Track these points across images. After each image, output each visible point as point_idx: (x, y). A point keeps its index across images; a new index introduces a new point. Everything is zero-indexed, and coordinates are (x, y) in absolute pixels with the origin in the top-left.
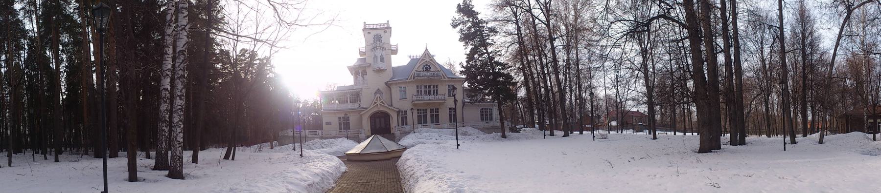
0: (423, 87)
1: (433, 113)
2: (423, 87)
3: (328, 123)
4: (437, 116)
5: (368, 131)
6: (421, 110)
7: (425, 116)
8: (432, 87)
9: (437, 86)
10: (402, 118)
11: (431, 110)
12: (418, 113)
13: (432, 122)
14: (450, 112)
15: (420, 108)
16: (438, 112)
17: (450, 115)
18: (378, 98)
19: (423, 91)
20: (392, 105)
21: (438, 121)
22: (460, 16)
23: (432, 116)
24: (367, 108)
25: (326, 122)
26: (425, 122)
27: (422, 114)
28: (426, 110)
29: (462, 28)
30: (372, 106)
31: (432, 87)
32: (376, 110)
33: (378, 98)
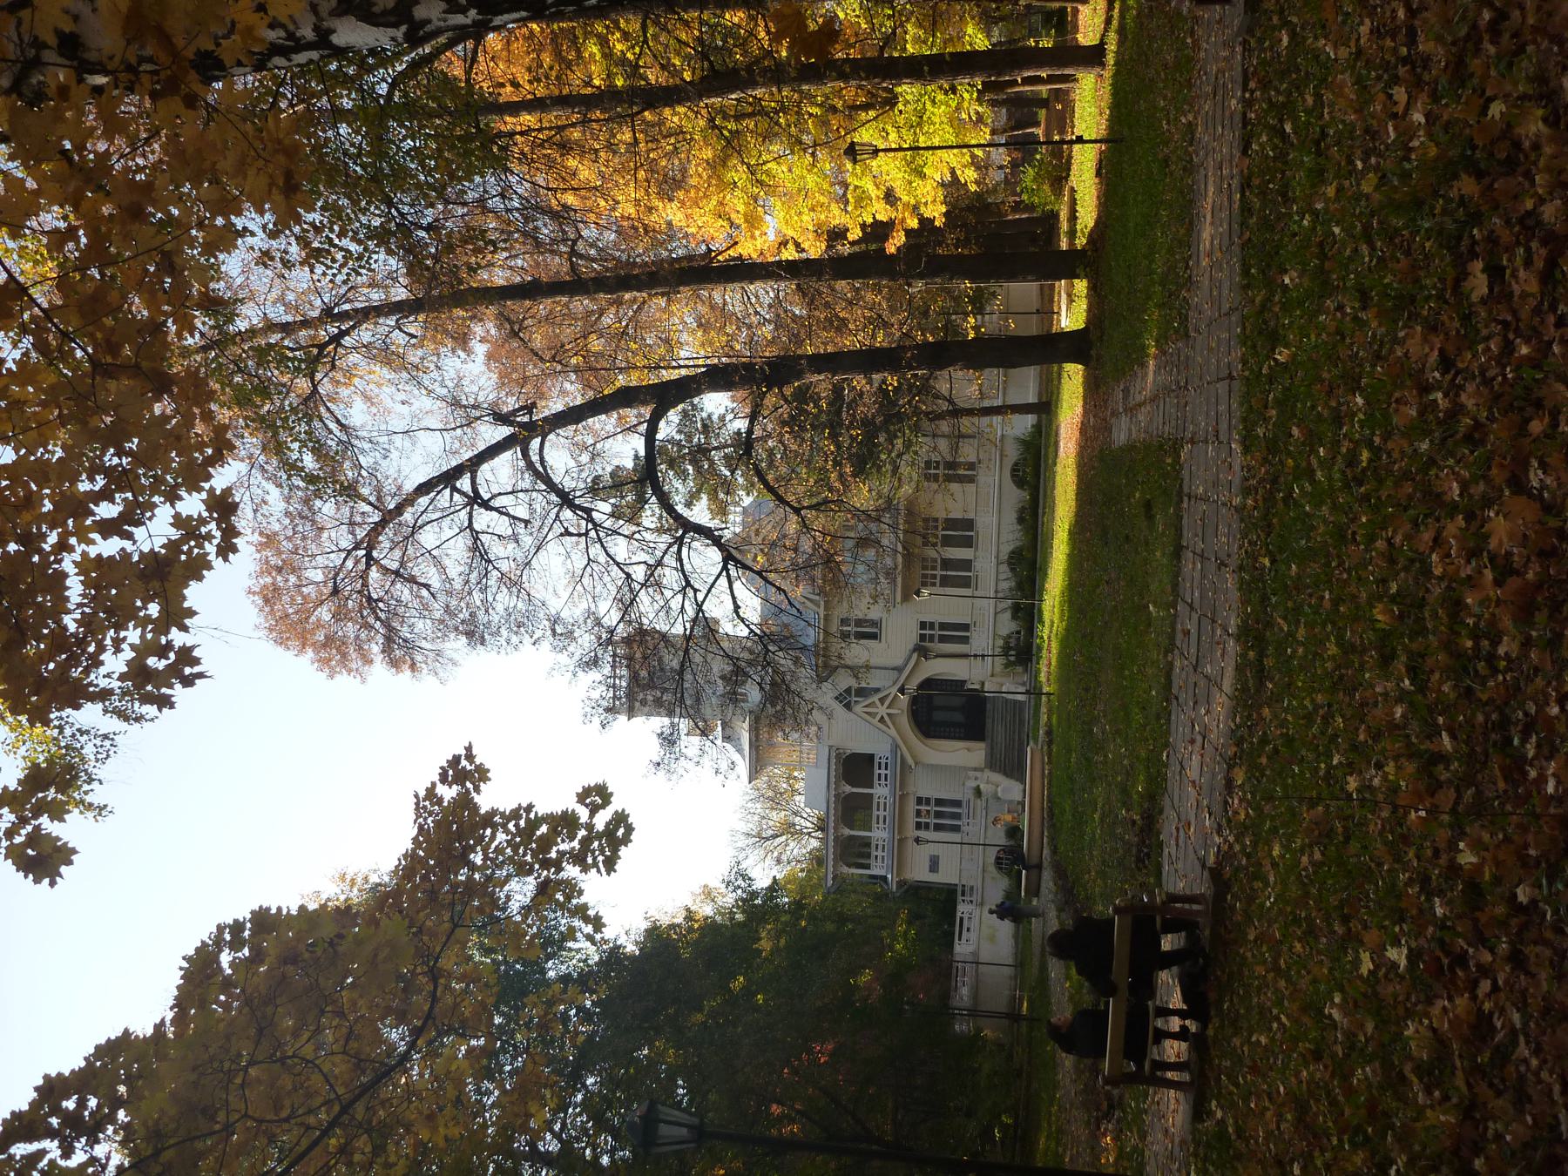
3: (934, 865)
4: (951, 523)
5: (968, 750)
10: (943, 639)
13: (968, 542)
16: (936, 520)
18: (866, 710)
20: (899, 670)
21: (969, 524)
23: (948, 542)
24: (897, 746)
26: (967, 565)
27: (939, 573)
30: (893, 732)
32: (904, 721)
33: (866, 710)
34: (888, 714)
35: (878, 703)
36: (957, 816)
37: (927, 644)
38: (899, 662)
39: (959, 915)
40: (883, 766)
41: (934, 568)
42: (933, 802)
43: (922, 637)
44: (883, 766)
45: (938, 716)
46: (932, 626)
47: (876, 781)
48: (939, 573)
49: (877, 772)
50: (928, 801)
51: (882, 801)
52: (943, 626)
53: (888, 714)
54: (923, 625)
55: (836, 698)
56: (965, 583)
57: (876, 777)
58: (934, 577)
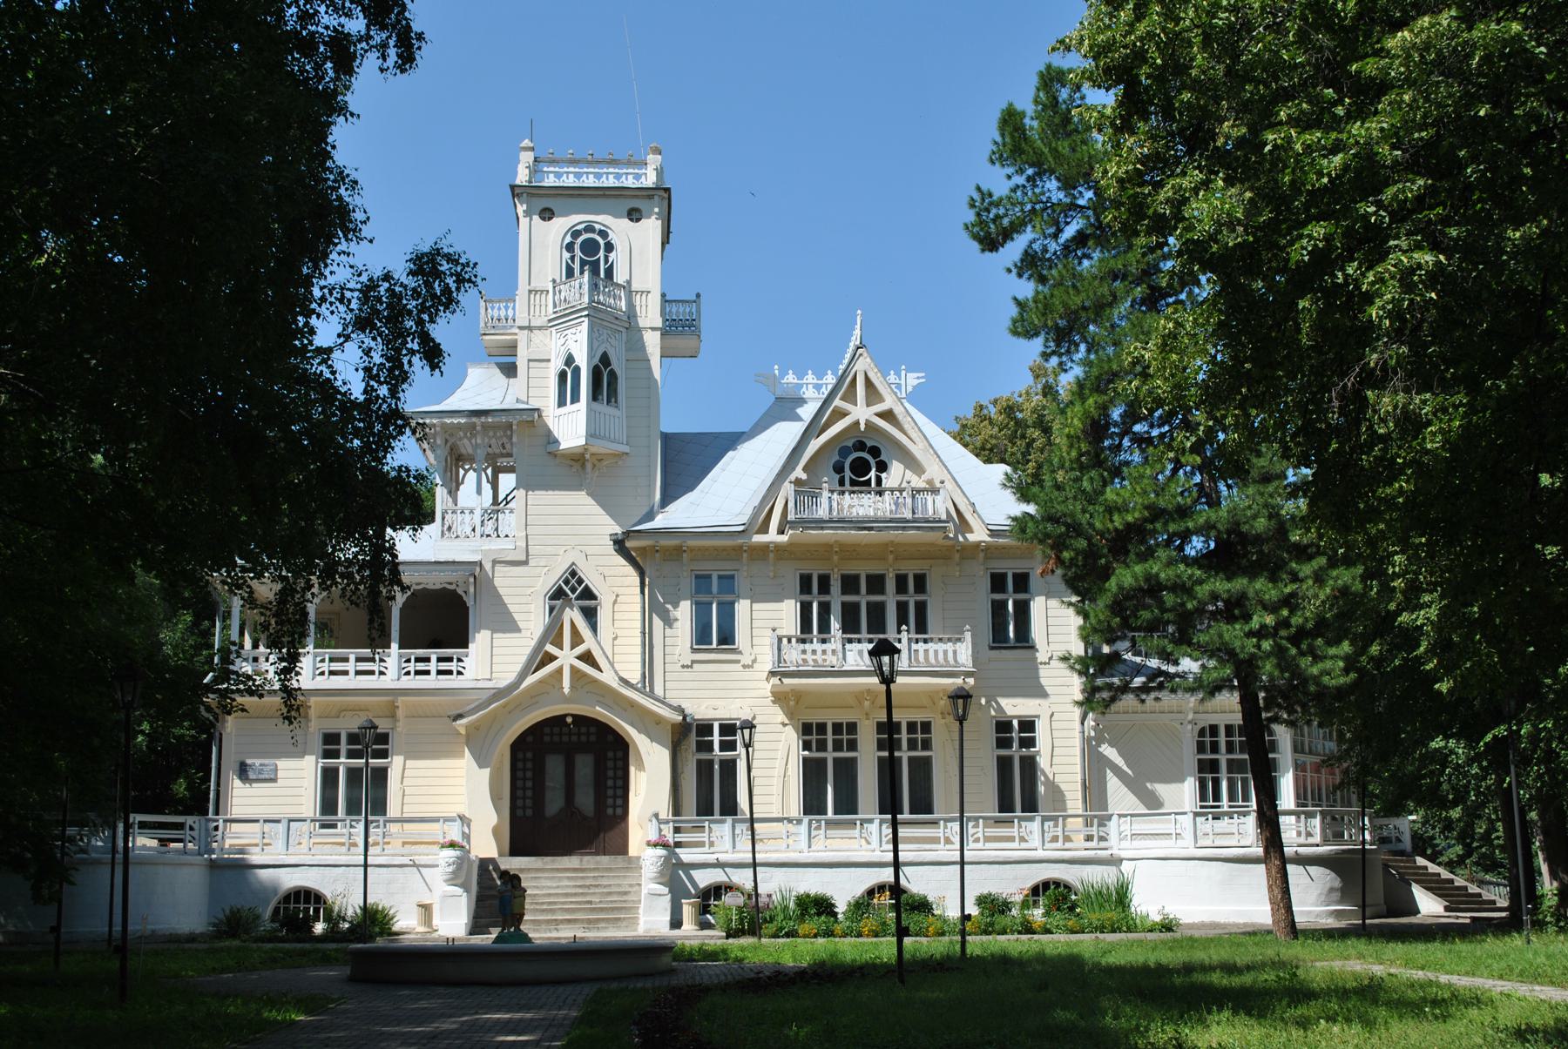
0: (836, 586)
2: (836, 586)
6: (822, 728)
7: (847, 772)
8: (890, 585)
9: (921, 585)
10: (704, 769)
12: (807, 746)
14: (1003, 743)
16: (927, 745)
17: (1004, 765)
19: (836, 609)
22: (1020, 180)
23: (889, 770)
26: (847, 804)
28: (852, 727)
29: (1036, 246)
31: (890, 585)
34: (560, 671)
35: (580, 650)
37: (693, 738)
38: (659, 691)
39: (189, 820)
40: (444, 666)
41: (838, 746)
44: (444, 666)
45: (554, 767)
49: (433, 654)
53: (560, 671)
55: (573, 574)
56: (813, 804)
57: (421, 652)
58: (822, 746)
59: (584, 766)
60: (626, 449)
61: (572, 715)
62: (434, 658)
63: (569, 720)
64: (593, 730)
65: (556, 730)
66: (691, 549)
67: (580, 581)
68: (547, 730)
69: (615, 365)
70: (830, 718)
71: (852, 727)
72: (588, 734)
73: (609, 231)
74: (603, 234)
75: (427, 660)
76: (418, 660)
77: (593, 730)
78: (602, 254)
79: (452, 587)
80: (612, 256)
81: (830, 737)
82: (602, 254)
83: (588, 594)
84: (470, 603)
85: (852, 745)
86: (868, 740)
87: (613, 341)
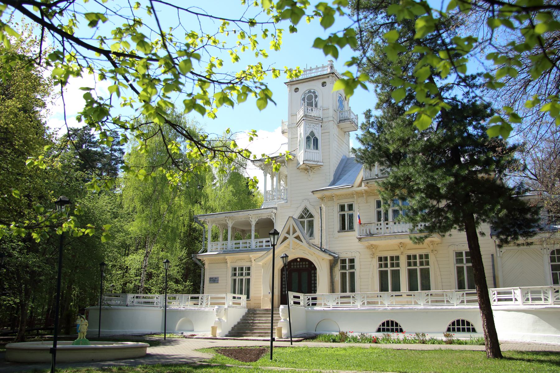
1: (415, 264)
4: (426, 274)
6: (386, 258)
7: (396, 275)
10: (343, 276)
11: (409, 257)
12: (381, 266)
13: (412, 287)
15: (383, 255)
16: (427, 263)
21: (426, 286)
23: (412, 274)
25: (210, 278)
26: (396, 287)
27: (389, 269)
28: (398, 258)
36: (344, 290)
37: (339, 265)
41: (392, 265)
42: (248, 277)
43: (344, 261)
45: (295, 275)
46: (352, 267)
47: (258, 240)
48: (389, 269)
50: (249, 274)
51: (248, 245)
52: (352, 275)
54: (352, 261)
57: (261, 240)
58: (386, 266)
59: (305, 275)
60: (321, 164)
61: (300, 258)
62: (264, 242)
63: (298, 260)
64: (307, 263)
65: (295, 264)
66: (337, 196)
67: (308, 211)
68: (292, 264)
69: (317, 135)
70: (389, 254)
71: (398, 258)
72: (305, 265)
73: (316, 92)
74: (314, 93)
75: (262, 242)
76: (260, 242)
77: (307, 263)
78: (313, 99)
79: (269, 217)
80: (317, 99)
81: (389, 262)
82: (313, 99)
83: (311, 216)
84: (274, 222)
85: (398, 265)
86: (403, 262)
87: (316, 127)
